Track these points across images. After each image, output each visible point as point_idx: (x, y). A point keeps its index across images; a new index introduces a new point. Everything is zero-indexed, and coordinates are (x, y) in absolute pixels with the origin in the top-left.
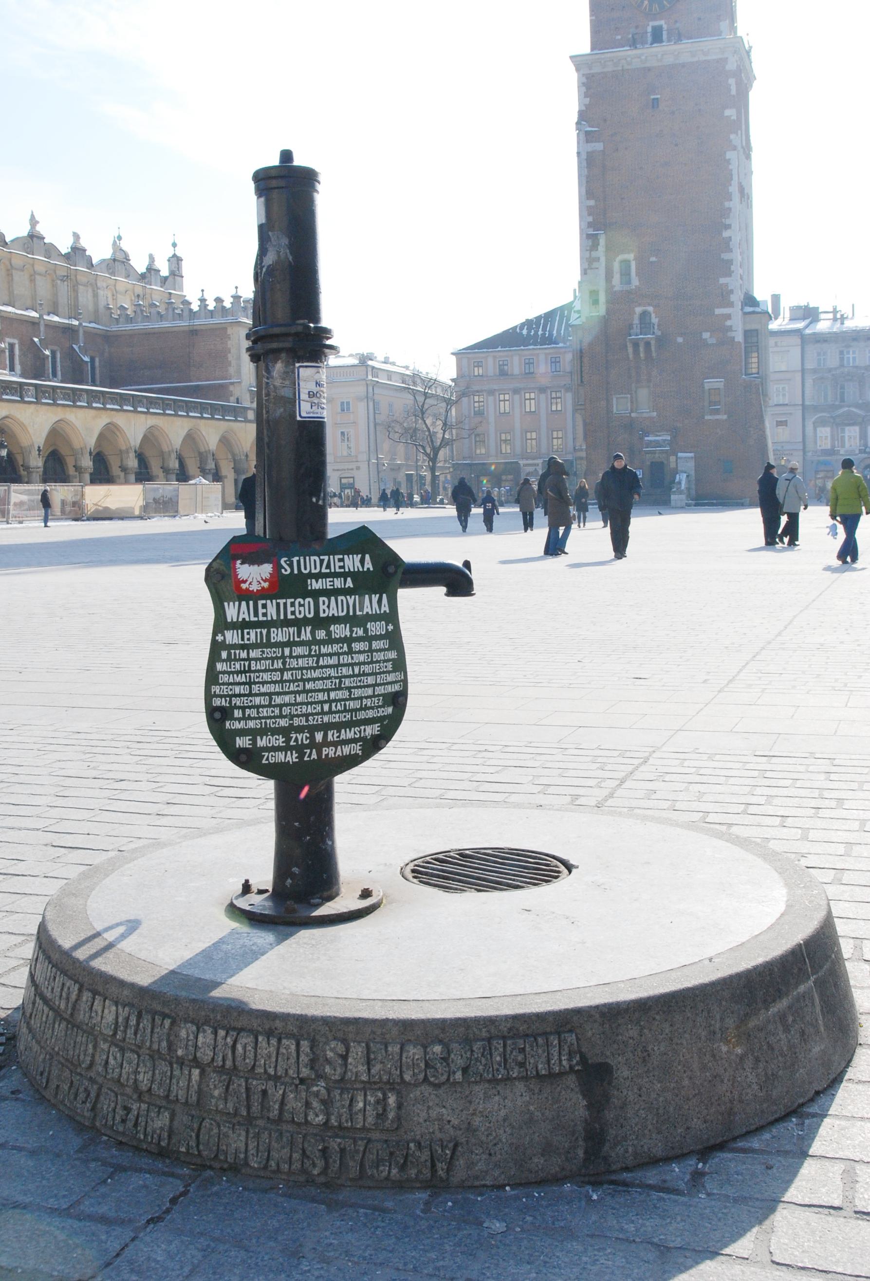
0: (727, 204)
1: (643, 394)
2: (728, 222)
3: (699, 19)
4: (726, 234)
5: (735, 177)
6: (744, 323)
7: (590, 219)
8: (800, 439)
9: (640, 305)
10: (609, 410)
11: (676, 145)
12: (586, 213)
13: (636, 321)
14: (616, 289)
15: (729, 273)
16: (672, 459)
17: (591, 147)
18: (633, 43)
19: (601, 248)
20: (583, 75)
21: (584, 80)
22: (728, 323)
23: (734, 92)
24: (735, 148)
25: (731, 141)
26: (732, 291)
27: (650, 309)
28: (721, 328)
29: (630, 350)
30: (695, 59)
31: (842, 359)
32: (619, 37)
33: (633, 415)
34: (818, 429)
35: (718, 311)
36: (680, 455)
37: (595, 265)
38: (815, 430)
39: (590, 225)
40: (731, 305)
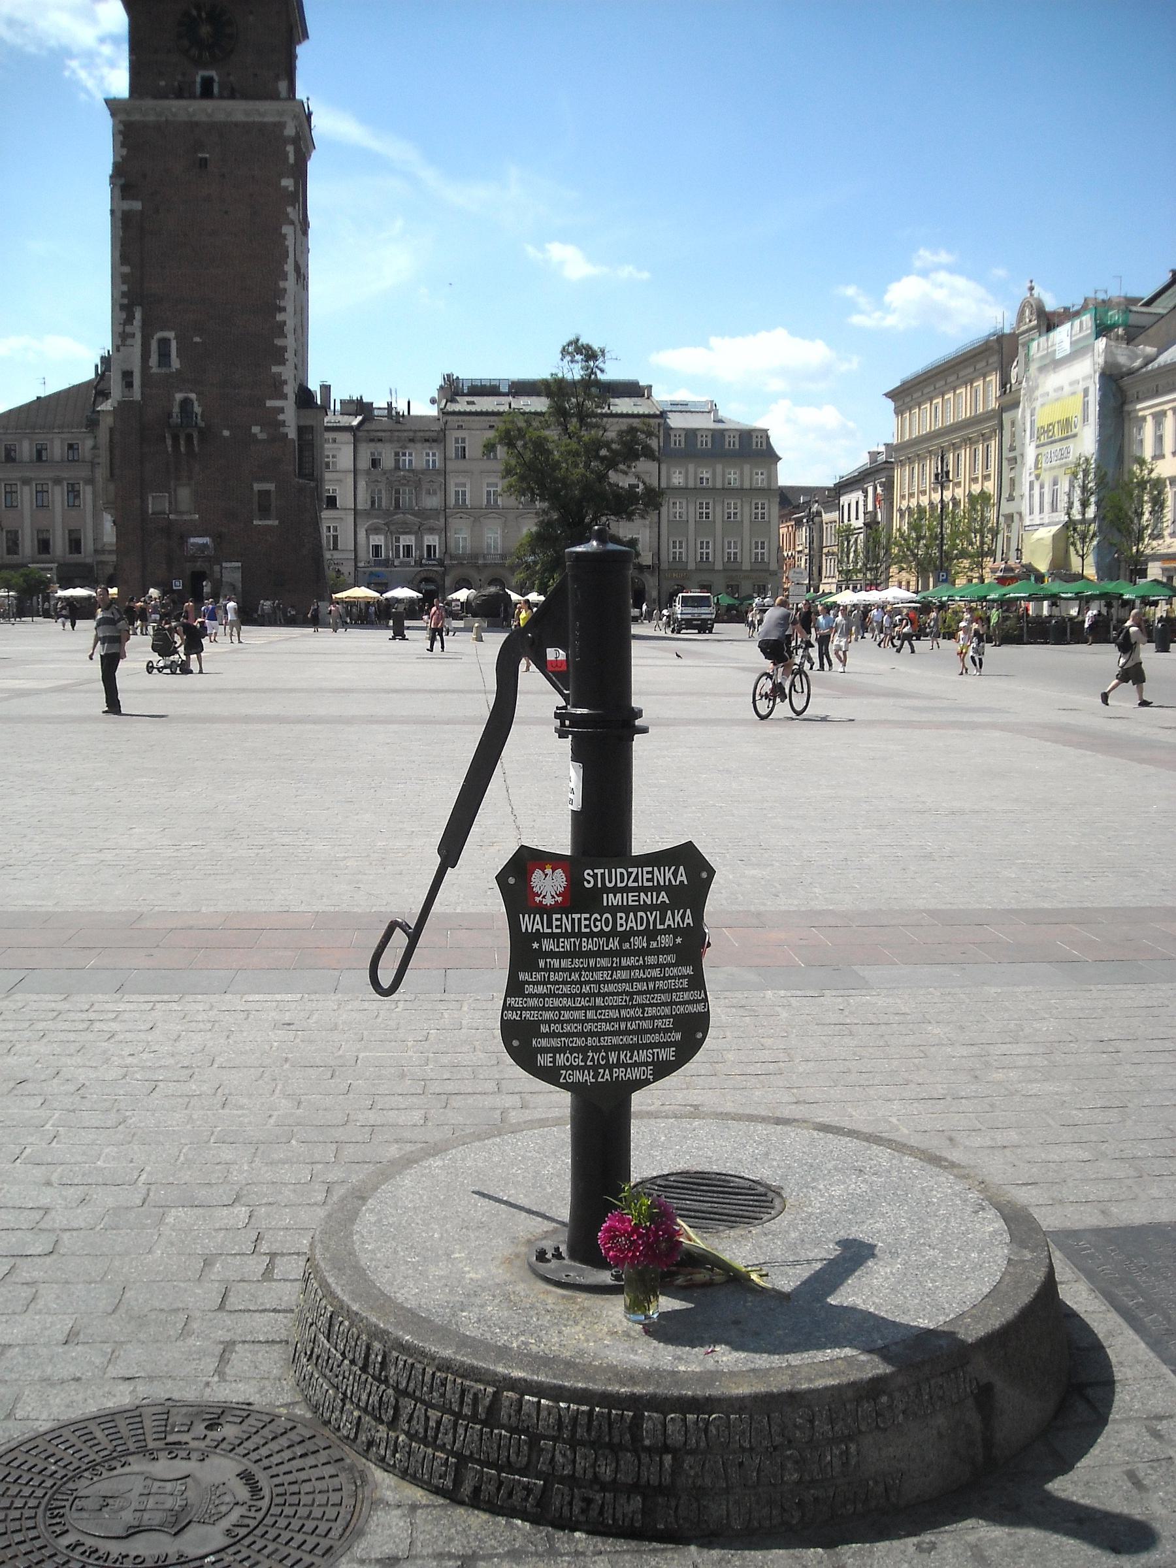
0: (282, 284)
2: (282, 304)
3: (256, 75)
4: (280, 317)
5: (291, 255)
6: (298, 417)
7: (125, 288)
9: (181, 391)
10: (143, 510)
11: (226, 212)
12: (119, 280)
13: (176, 410)
14: (154, 370)
15: (282, 362)
16: (217, 568)
17: (128, 205)
18: (180, 94)
19: (135, 323)
20: (120, 122)
21: (121, 127)
22: (281, 417)
23: (292, 160)
24: (292, 223)
25: (288, 214)
26: (285, 382)
27: (193, 396)
28: (273, 422)
29: (169, 442)
30: (251, 119)
31: (397, 461)
32: (162, 83)
33: (171, 517)
35: (269, 403)
36: (224, 564)
37: (129, 341)
38: (368, 538)
40: (284, 397)
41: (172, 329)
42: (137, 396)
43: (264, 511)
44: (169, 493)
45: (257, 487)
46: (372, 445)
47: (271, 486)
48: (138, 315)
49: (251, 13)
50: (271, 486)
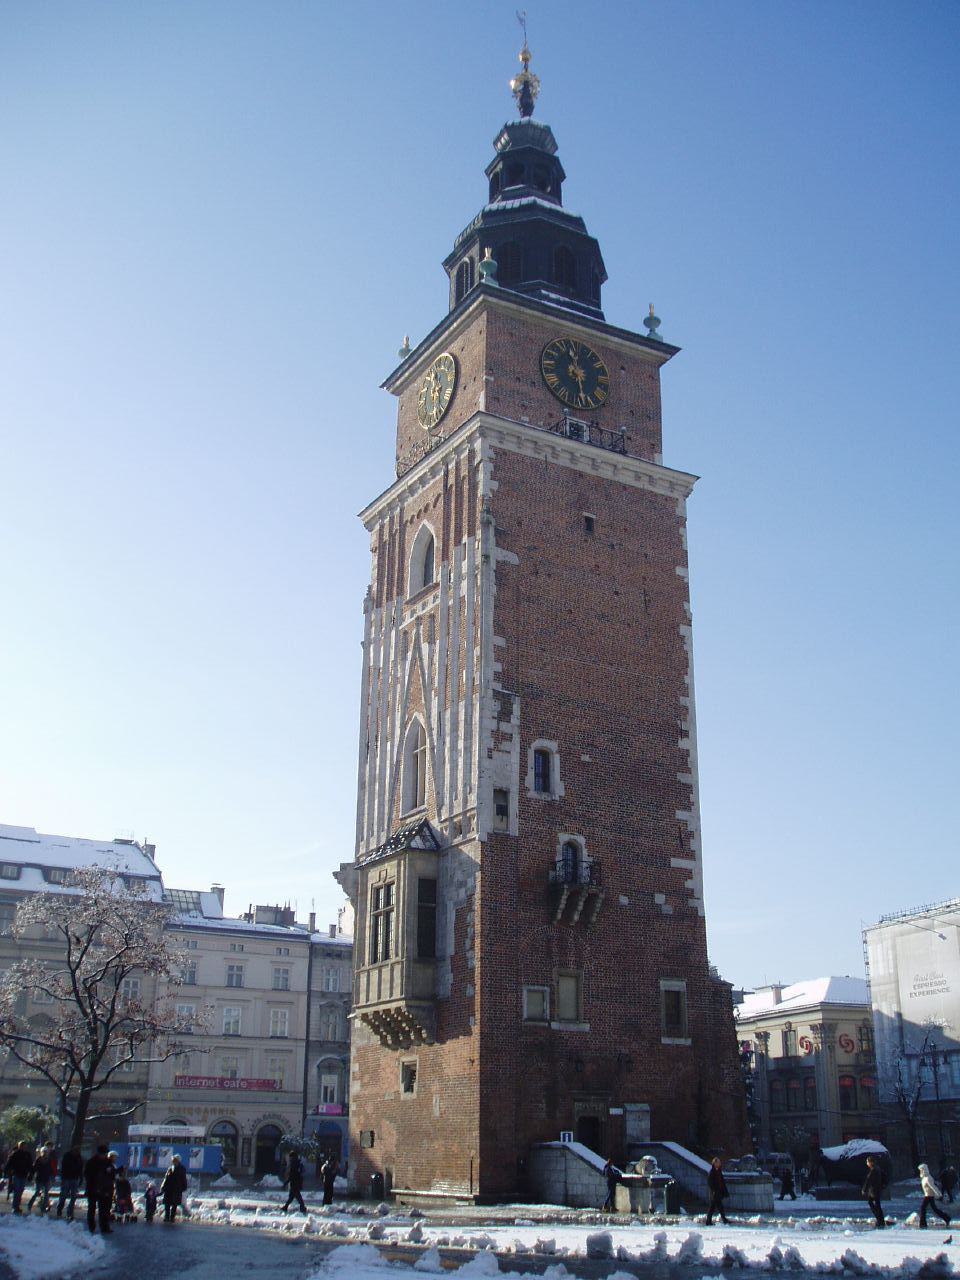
0: (683, 700)
1: (567, 988)
4: (683, 744)
7: (499, 667)
8: (301, 1089)
11: (617, 593)
14: (532, 794)
21: (494, 456)
22: (689, 884)
27: (581, 840)
33: (555, 1025)
34: (323, 1077)
35: (676, 862)
37: (505, 745)
38: (320, 1077)
39: (497, 676)
41: (552, 738)
42: (514, 827)
43: (674, 1025)
44: (551, 986)
45: (665, 985)
46: (328, 960)
47: (678, 985)
48: (516, 709)
49: (623, 368)
50: (678, 985)
